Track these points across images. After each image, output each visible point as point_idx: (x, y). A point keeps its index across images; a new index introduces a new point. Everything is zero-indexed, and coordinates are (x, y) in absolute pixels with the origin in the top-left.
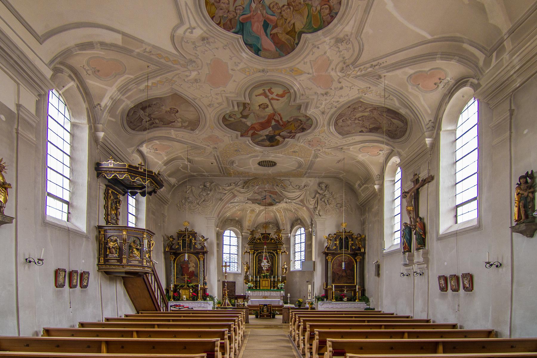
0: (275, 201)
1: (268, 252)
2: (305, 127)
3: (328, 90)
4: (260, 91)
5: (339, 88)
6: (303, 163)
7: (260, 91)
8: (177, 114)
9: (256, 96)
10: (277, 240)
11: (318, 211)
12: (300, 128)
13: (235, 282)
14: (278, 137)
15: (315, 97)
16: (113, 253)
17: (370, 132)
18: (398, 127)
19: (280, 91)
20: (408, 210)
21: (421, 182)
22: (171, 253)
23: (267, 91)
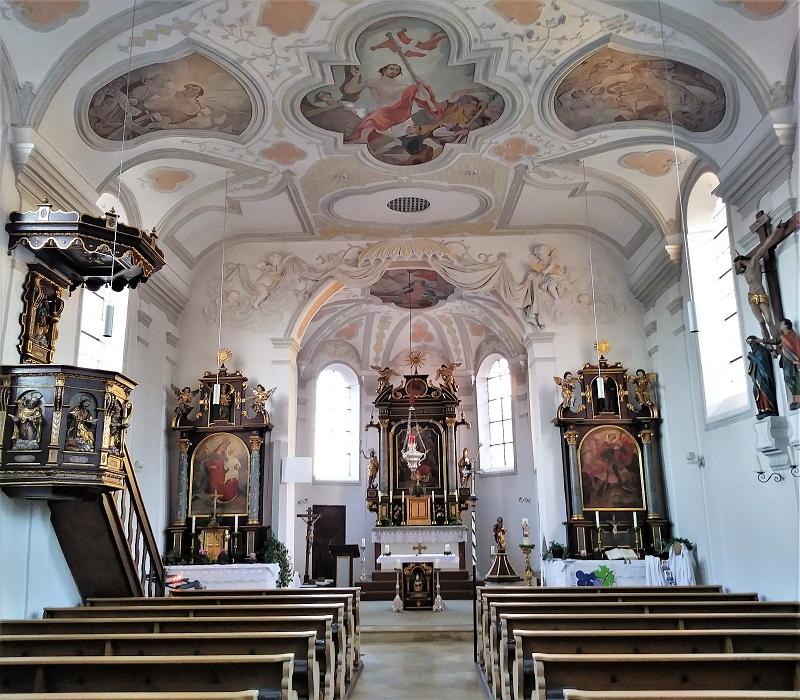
0: (434, 295)
1: (422, 425)
2: (487, 113)
3: (532, 27)
4: (381, 37)
5: (557, 21)
6: (491, 201)
7: (381, 37)
8: (200, 99)
9: (373, 49)
10: (443, 391)
12: (476, 117)
13: (344, 507)
14: (428, 142)
15: (505, 44)
16: (25, 438)
17: (640, 118)
18: (703, 103)
19: (424, 35)
20: (754, 302)
21: (777, 232)
22: (182, 433)
23: (396, 37)
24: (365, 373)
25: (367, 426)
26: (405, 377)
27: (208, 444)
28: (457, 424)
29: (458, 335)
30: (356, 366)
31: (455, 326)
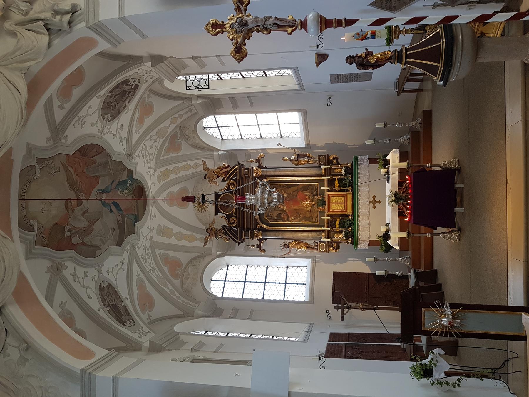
0: (125, 182)
11: (58, 17)
24: (213, 251)
25: (261, 250)
26: (216, 214)
28: (260, 166)
29: (180, 165)
30: (207, 259)
31: (171, 167)
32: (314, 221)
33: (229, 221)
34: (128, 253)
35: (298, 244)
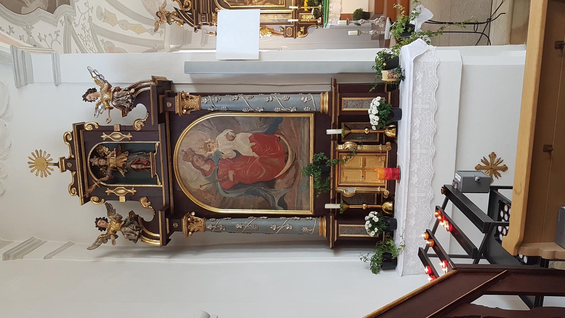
24: (166, 45)
27: (194, 186)
32: (280, 4)
33: (183, 5)
34: (63, 25)
35: (262, 29)
